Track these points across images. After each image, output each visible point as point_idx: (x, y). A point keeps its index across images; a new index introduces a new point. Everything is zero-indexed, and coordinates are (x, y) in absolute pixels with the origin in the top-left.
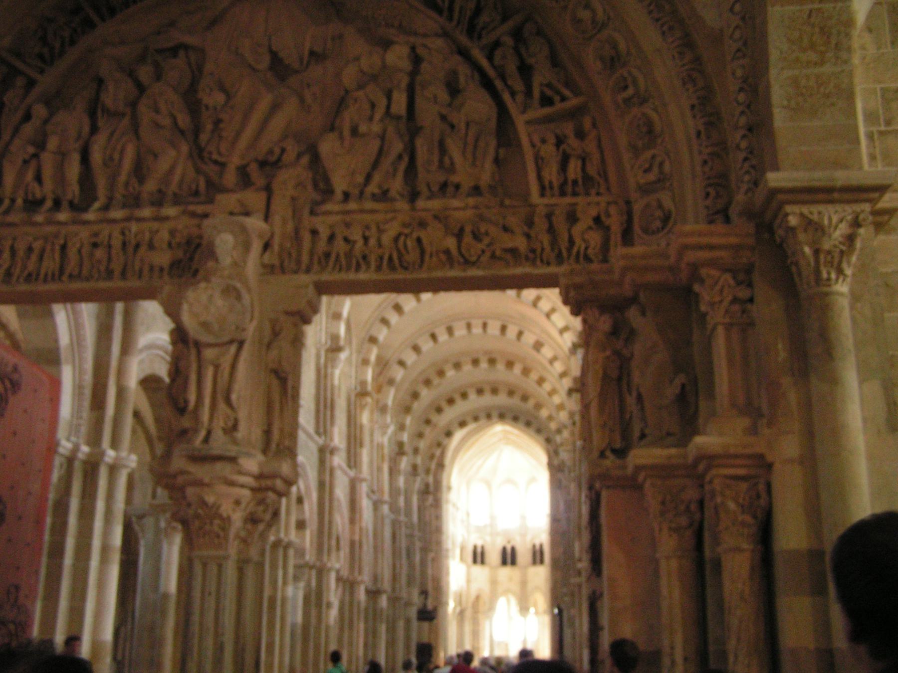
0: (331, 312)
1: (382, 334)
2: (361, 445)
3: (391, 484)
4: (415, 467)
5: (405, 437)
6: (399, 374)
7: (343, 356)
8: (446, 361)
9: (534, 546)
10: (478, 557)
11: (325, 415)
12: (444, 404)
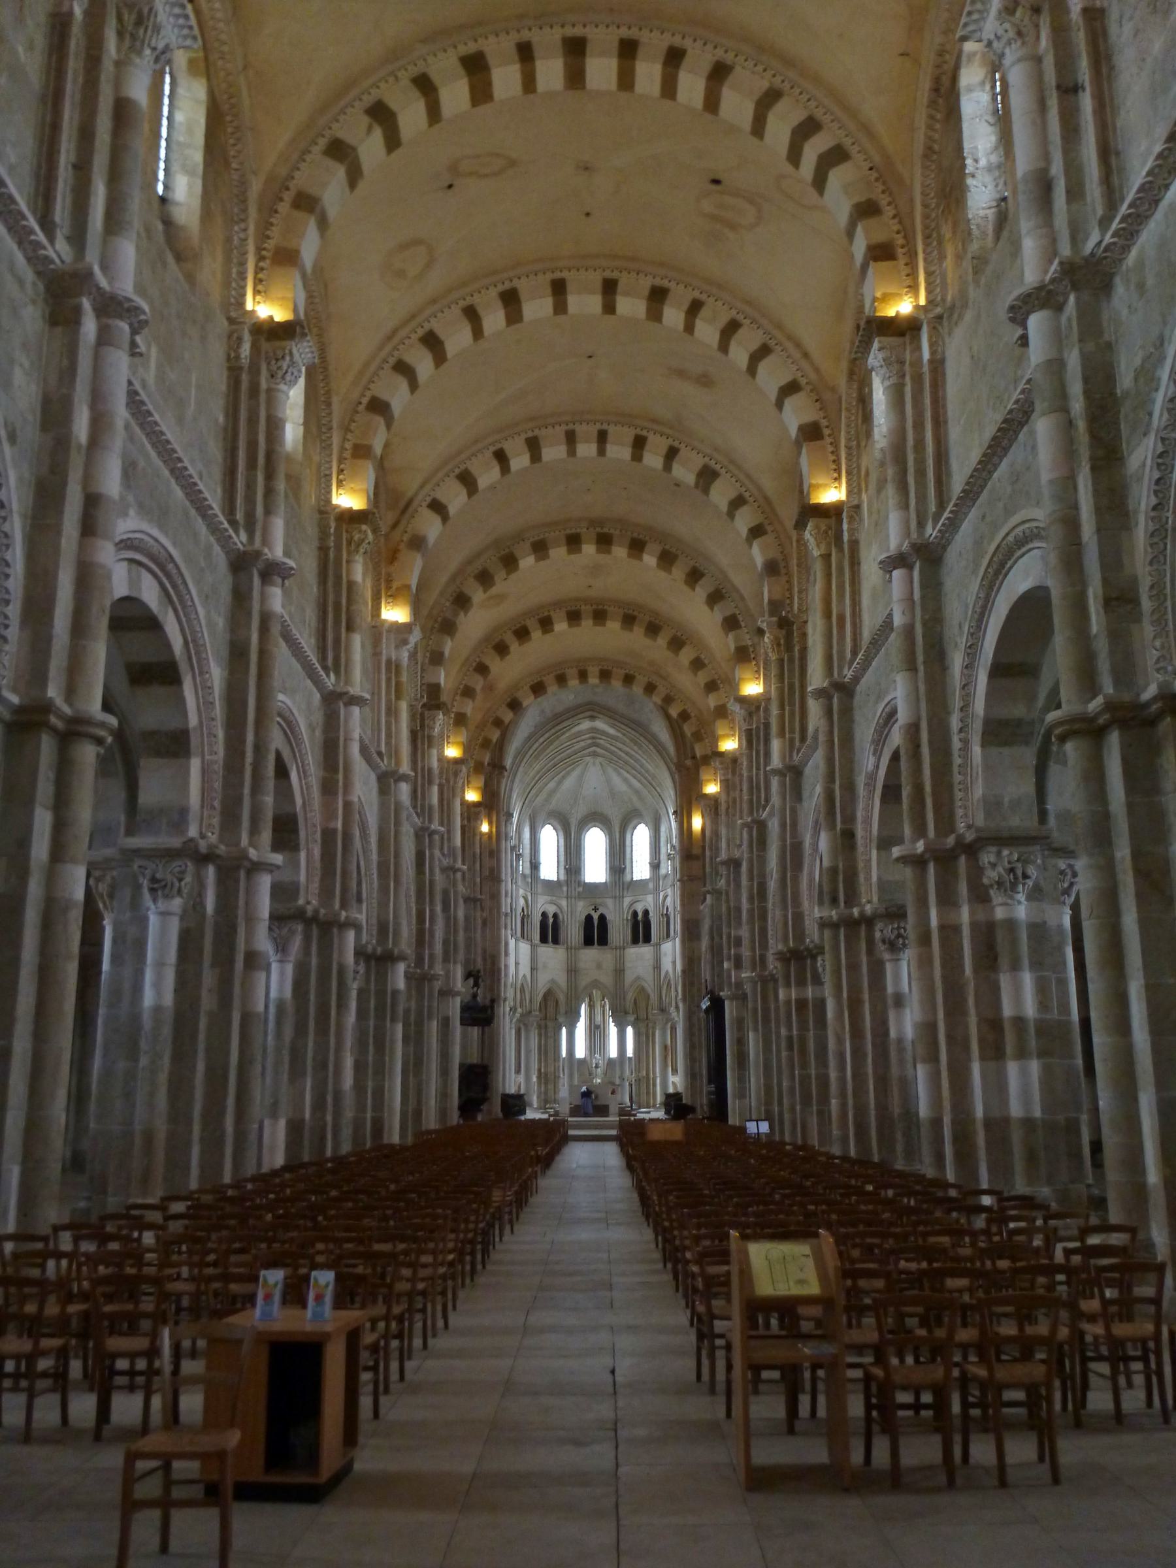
0: (270, 244)
1: (398, 396)
2: (350, 628)
6: (431, 527)
8: (519, 537)
10: (550, 931)
11: (250, 486)
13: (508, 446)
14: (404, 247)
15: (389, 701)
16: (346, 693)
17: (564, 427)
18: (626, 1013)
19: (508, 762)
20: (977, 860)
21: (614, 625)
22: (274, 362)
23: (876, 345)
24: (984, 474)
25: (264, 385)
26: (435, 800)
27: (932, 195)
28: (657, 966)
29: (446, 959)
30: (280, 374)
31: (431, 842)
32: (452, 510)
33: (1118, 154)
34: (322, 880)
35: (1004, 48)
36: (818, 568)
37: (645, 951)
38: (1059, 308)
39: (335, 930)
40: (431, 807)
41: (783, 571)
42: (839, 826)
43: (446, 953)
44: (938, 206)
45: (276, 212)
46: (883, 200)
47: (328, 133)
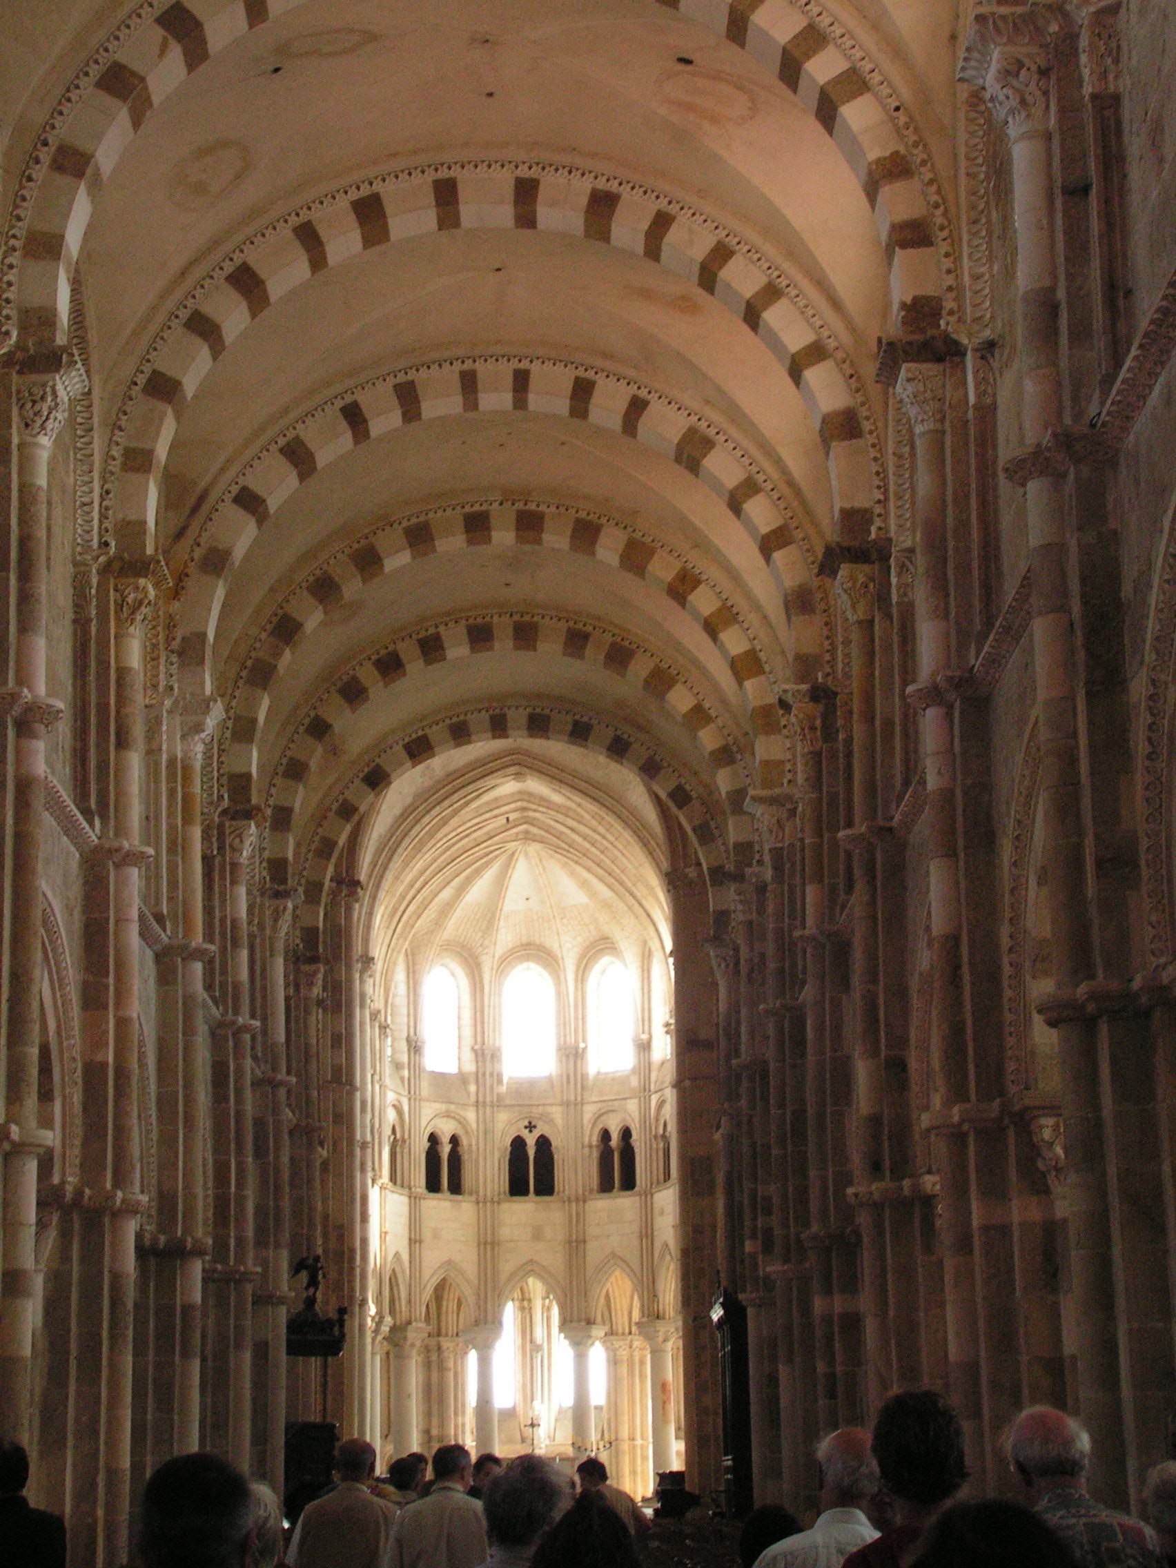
2: (122, 743)
3: (208, 910)
4: (277, 868)
5: (254, 761)
7: (68, 385)
9: (606, 1135)
12: (368, 674)
13: (364, 399)
14: (204, 151)
15: (172, 828)
16: (118, 850)
17: (458, 366)
18: (590, 1322)
19: (363, 877)
20: (1030, 1133)
21: (550, 648)
22: (29, 405)
23: (903, 374)
24: (1023, 613)
25: (15, 440)
26: (244, 975)
27: (980, 161)
28: (647, 1233)
29: (261, 1242)
30: (39, 422)
31: (236, 1046)
32: (273, 504)
33: (1129, 293)
34: (86, 1143)
35: (1007, 116)
36: (855, 635)
37: (624, 1204)
38: (1061, 476)
39: (107, 1220)
40: (237, 986)
41: (820, 606)
42: (883, 1052)
43: (261, 1230)
44: (988, 178)
45: (30, 179)
46: (918, 155)
47: (103, 57)
